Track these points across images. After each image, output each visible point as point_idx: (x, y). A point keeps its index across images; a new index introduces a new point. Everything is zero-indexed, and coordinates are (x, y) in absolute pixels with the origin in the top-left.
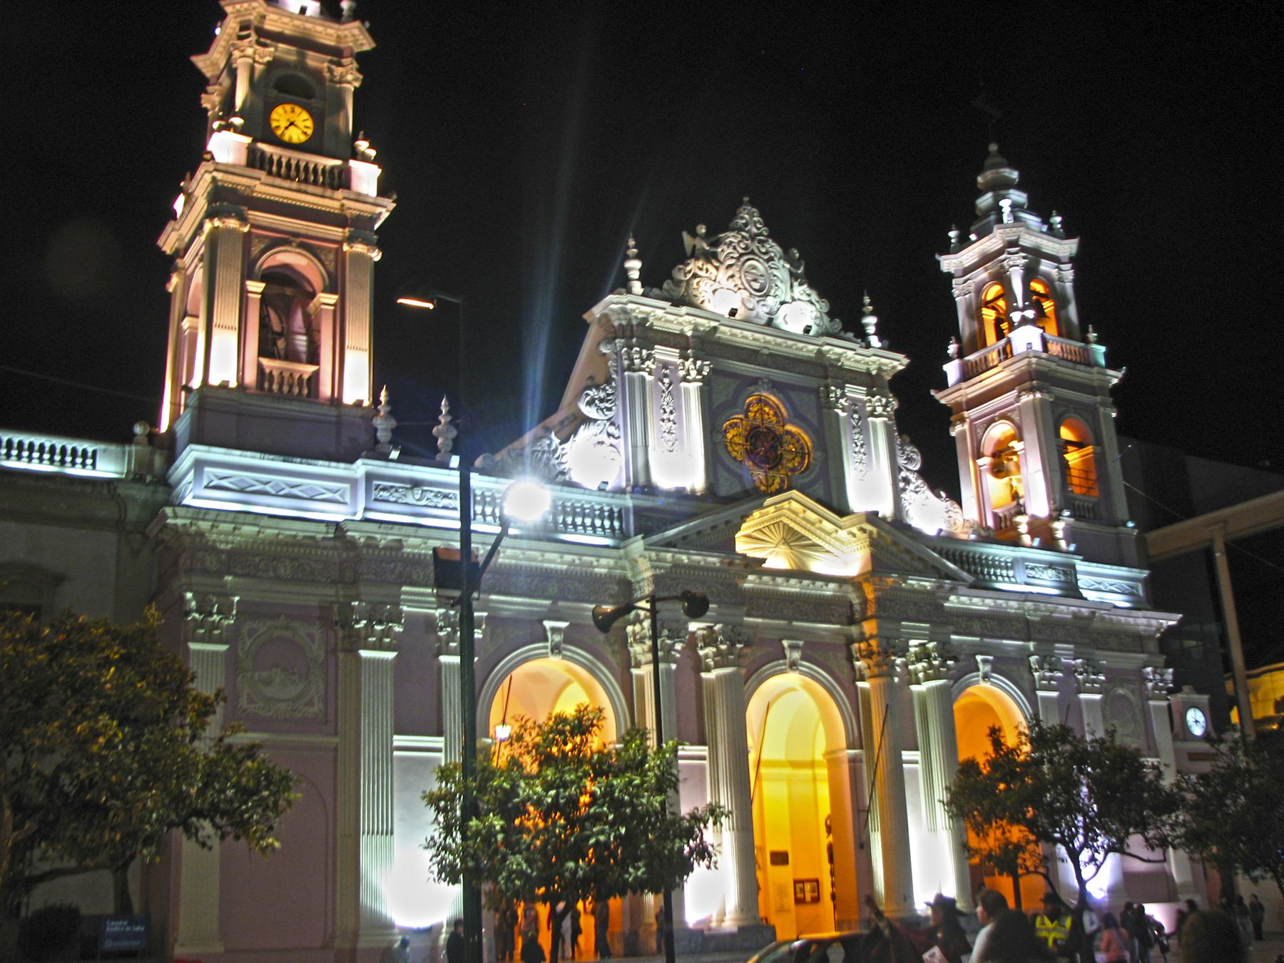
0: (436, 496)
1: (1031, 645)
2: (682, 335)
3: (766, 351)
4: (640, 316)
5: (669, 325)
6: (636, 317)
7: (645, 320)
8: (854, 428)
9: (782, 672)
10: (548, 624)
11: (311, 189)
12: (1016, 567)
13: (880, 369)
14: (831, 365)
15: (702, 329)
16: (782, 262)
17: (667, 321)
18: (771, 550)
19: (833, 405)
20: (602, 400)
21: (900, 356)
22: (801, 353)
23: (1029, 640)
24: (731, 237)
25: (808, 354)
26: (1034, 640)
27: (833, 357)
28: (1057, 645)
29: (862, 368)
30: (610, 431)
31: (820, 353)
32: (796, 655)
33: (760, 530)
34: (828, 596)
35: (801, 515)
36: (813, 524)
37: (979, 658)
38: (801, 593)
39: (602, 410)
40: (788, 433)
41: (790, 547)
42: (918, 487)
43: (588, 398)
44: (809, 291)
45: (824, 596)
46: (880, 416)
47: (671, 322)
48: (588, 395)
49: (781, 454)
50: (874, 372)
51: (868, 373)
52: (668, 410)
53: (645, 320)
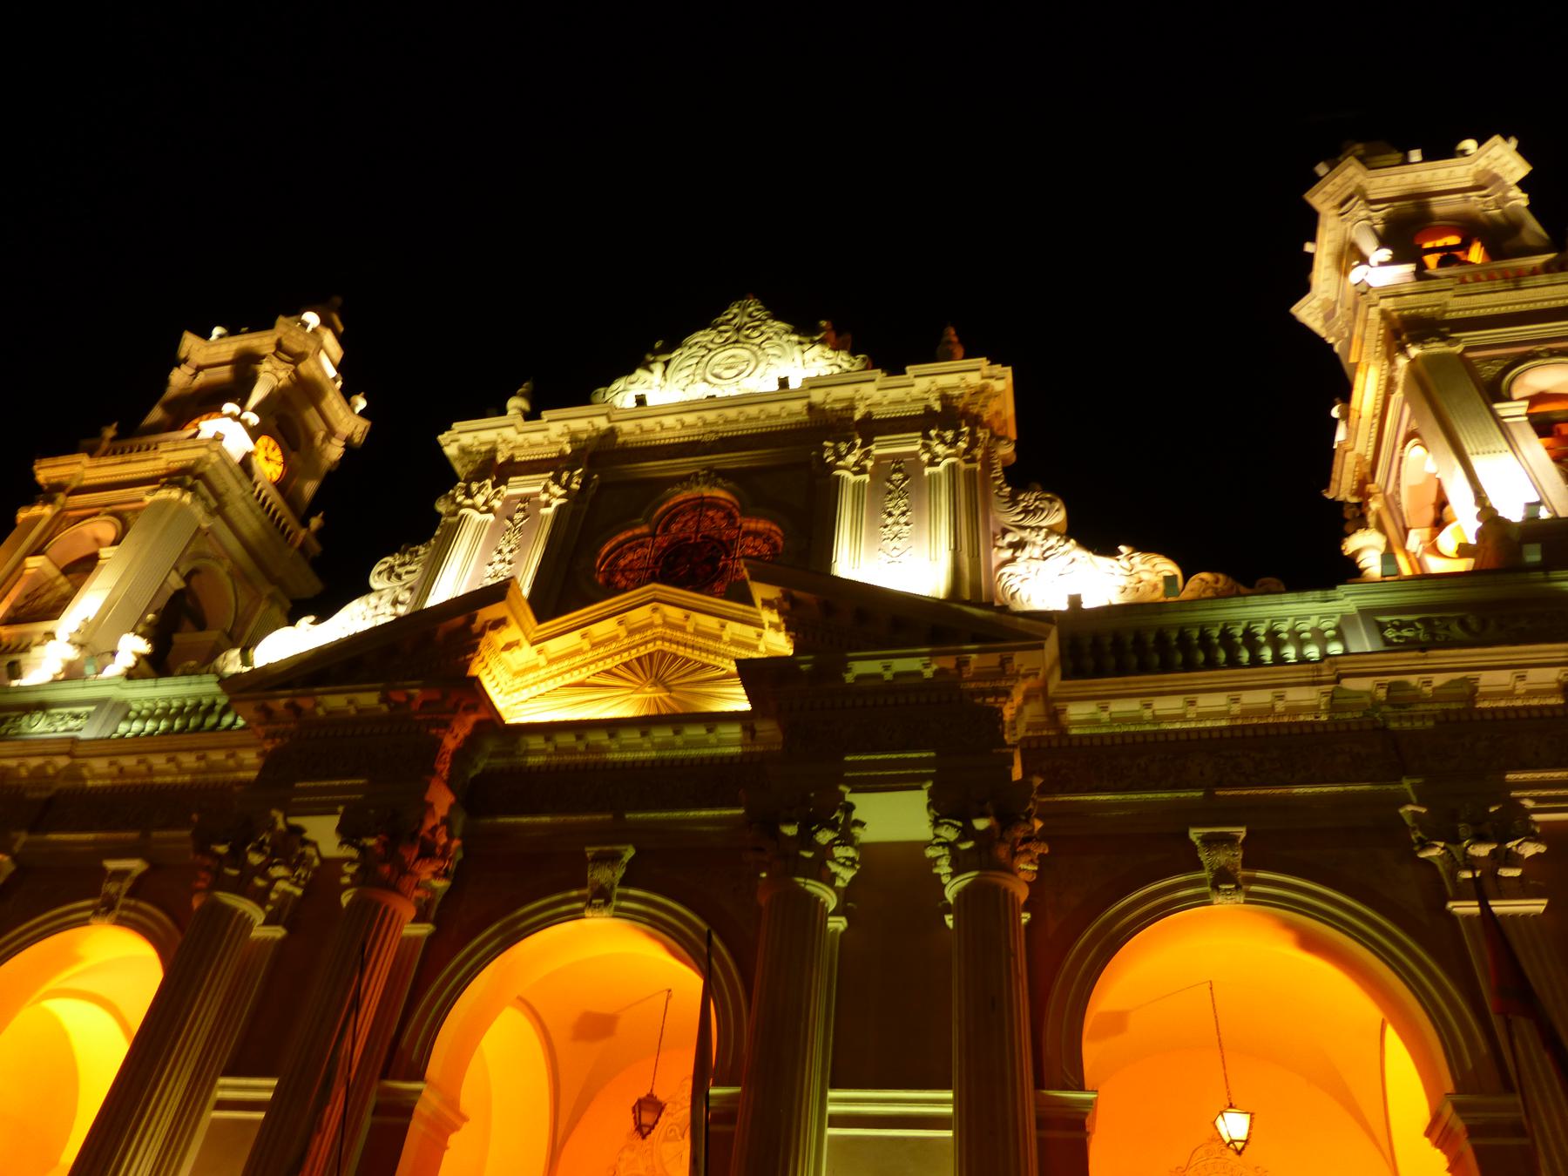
0: (62, 719)
1: (1407, 784)
2: (562, 456)
3: (713, 437)
4: (484, 448)
5: (536, 450)
6: (479, 452)
7: (493, 452)
8: (890, 492)
9: (576, 915)
10: (112, 865)
11: (134, 457)
12: (1348, 634)
13: (945, 397)
14: (840, 419)
15: (585, 436)
16: (785, 337)
17: (532, 446)
18: (625, 698)
19: (833, 467)
20: (403, 565)
21: (982, 362)
22: (780, 422)
23: (1398, 780)
24: (701, 337)
25: (794, 419)
26: (1410, 774)
27: (838, 406)
28: (1510, 777)
29: (918, 409)
30: (401, 598)
31: (811, 408)
32: (603, 875)
33: (608, 672)
34: (732, 757)
35: (690, 629)
36: (718, 638)
37: (1195, 834)
38: (662, 761)
39: (399, 577)
40: (747, 533)
41: (668, 689)
42: (1051, 548)
43: (383, 567)
44: (830, 354)
45: (722, 758)
46: (947, 457)
47: (541, 445)
48: (386, 563)
49: (725, 566)
50: (937, 407)
51: (929, 410)
52: (506, 550)
53: (493, 452)
